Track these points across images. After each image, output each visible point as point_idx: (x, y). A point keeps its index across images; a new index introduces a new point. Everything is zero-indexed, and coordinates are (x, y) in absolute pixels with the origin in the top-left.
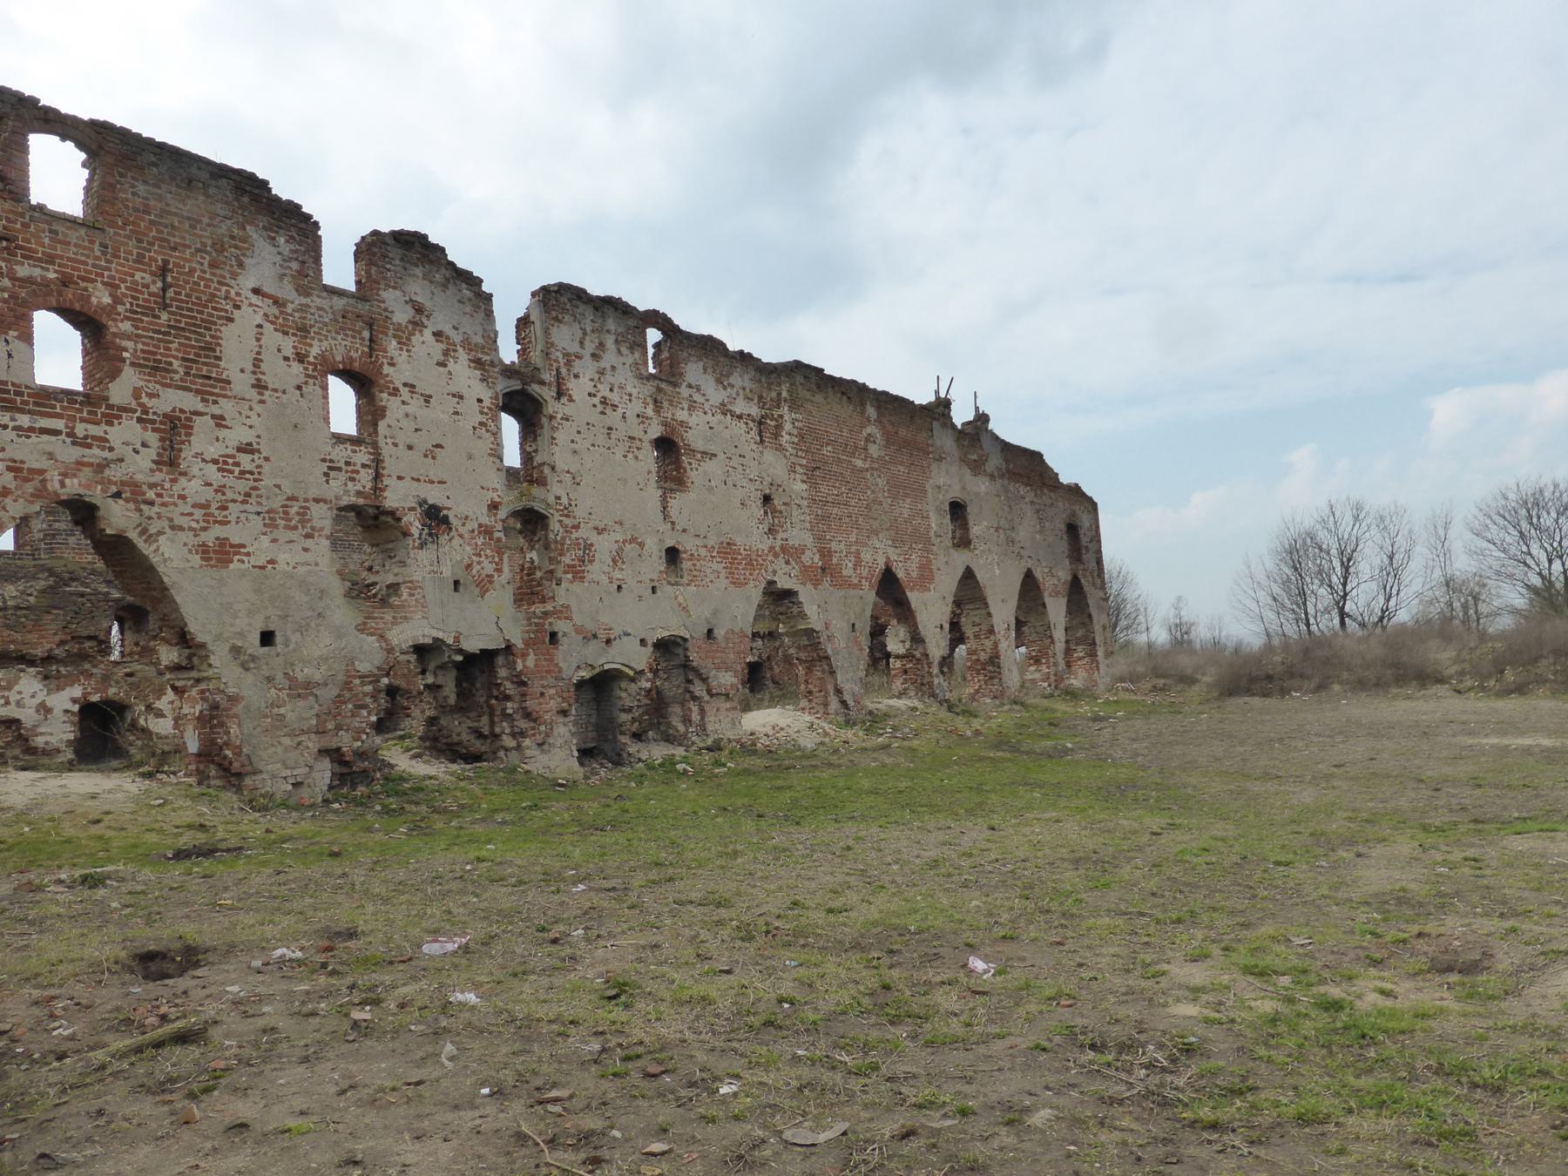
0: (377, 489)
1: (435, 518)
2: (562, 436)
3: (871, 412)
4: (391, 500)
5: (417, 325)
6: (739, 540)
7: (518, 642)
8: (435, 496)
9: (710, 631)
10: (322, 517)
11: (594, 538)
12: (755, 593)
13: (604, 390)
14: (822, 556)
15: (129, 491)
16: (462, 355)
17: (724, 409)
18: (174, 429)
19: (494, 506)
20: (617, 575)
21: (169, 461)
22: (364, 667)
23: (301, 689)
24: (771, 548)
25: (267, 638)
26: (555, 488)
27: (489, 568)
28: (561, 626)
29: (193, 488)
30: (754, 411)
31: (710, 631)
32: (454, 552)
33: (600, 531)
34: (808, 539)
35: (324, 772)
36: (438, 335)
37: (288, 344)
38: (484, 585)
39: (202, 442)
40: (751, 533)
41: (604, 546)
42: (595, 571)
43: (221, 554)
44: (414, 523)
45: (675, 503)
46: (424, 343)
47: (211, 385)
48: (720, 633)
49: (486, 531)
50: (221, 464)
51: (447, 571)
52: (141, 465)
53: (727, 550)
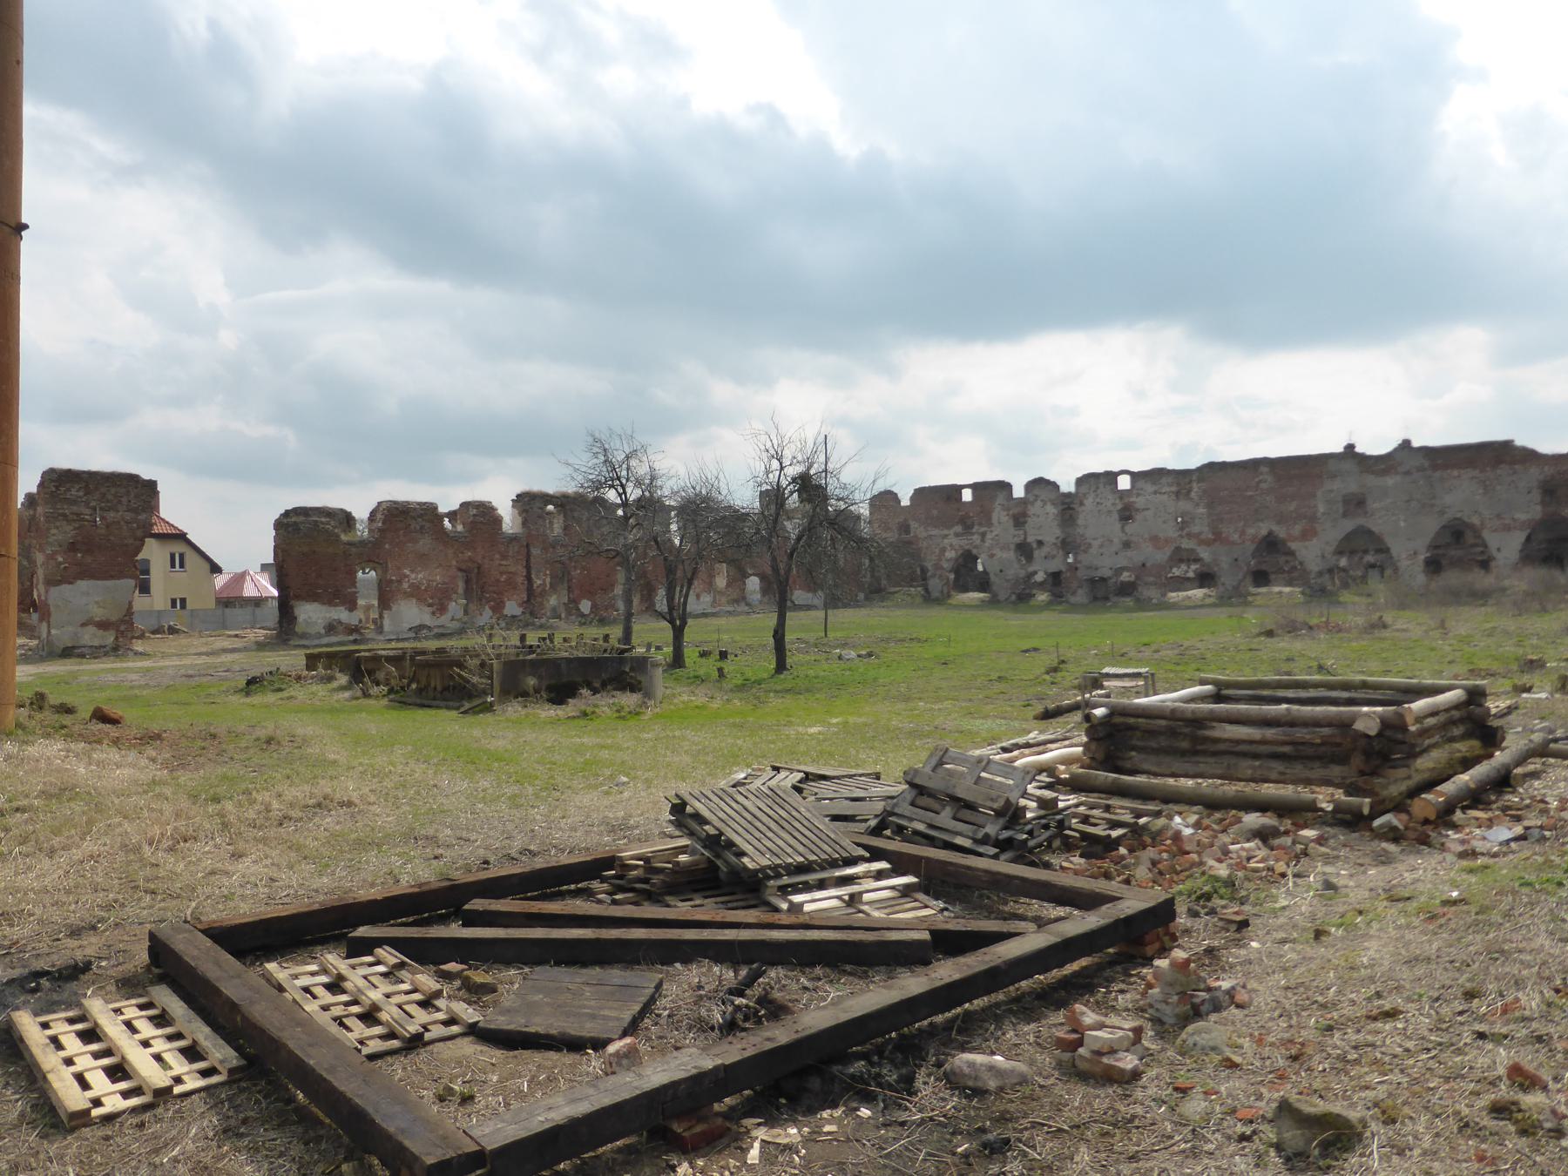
0: (1025, 539)
1: (1040, 543)
2: (1081, 516)
3: (1264, 469)
4: (1029, 540)
5: (1036, 500)
6: (1161, 535)
7: (1064, 570)
8: (1040, 538)
9: (1144, 565)
10: (1013, 547)
11: (1092, 542)
12: (1168, 551)
13: (1098, 500)
14: (1213, 534)
15: (976, 547)
16: (1049, 504)
17: (1155, 493)
18: (983, 535)
19: (1057, 538)
20: (1101, 551)
21: (983, 540)
22: (1021, 576)
23: (1007, 581)
24: (1181, 536)
25: (1001, 571)
26: (1078, 530)
27: (1055, 552)
28: (1078, 565)
29: (987, 544)
30: (1174, 489)
31: (1144, 565)
32: (1045, 550)
33: (1094, 539)
34: (1206, 529)
35: (1014, 597)
36: (1042, 501)
37: (1005, 513)
38: (1054, 557)
39: (989, 536)
40: (1171, 532)
41: (1096, 544)
42: (1091, 550)
43: (992, 556)
44: (1035, 546)
45: (1128, 529)
46: (1039, 503)
47: (990, 524)
48: (1148, 565)
49: (1055, 544)
50: (992, 539)
51: (1043, 555)
52: (978, 542)
53: (1154, 539)
